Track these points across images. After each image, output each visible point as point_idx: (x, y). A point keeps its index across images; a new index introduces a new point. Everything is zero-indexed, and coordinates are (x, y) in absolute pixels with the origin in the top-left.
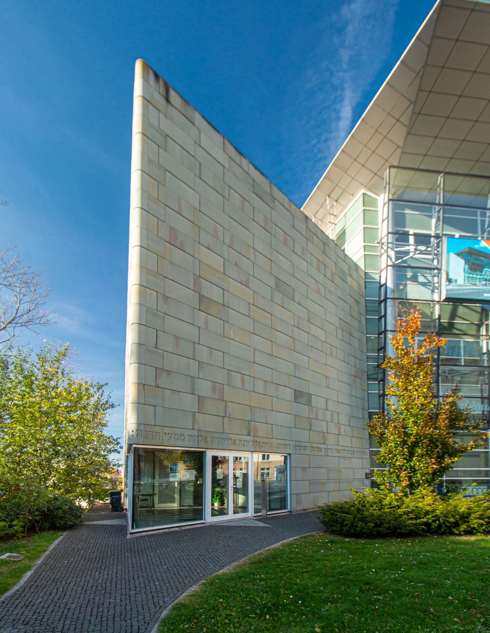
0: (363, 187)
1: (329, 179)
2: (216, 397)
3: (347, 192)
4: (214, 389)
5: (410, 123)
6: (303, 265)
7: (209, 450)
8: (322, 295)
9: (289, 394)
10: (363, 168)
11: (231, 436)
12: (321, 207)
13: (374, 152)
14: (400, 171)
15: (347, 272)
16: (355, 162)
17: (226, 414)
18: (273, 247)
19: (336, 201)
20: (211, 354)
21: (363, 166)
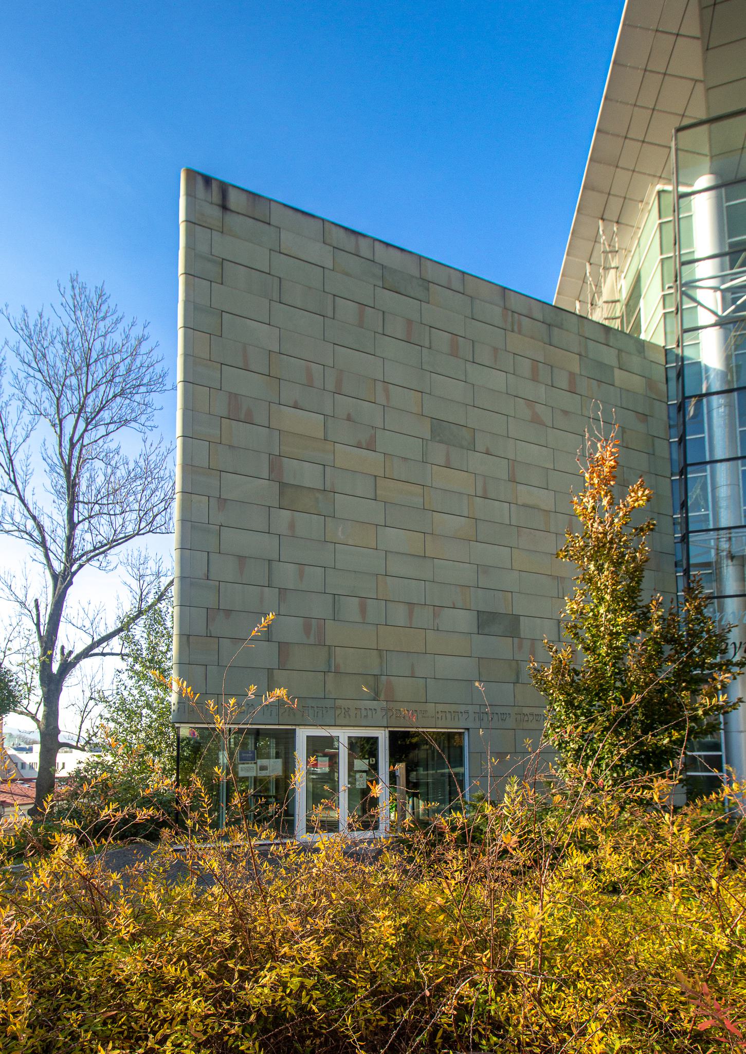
0: (657, 179)
1: (593, 189)
2: (312, 640)
3: (630, 199)
4: (307, 629)
5: (702, 31)
6: (498, 380)
7: (301, 727)
8: (544, 425)
9: (464, 620)
10: (645, 145)
11: (339, 702)
12: (595, 242)
13: (654, 110)
14: (715, 126)
15: (614, 362)
16: (627, 141)
17: (330, 666)
18: (425, 367)
19: (617, 222)
20: (301, 575)
21: (643, 142)
